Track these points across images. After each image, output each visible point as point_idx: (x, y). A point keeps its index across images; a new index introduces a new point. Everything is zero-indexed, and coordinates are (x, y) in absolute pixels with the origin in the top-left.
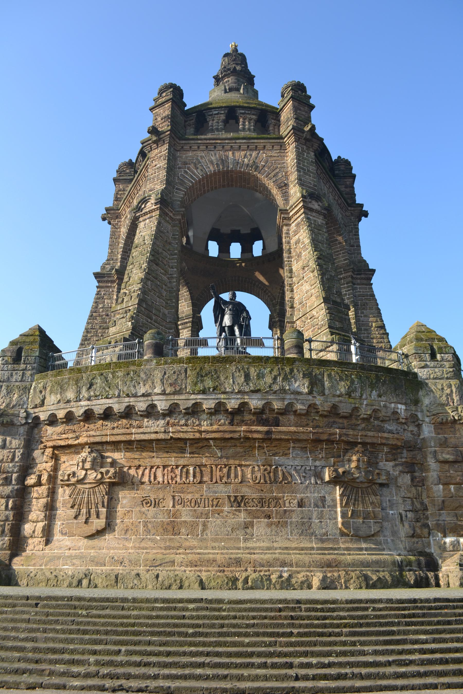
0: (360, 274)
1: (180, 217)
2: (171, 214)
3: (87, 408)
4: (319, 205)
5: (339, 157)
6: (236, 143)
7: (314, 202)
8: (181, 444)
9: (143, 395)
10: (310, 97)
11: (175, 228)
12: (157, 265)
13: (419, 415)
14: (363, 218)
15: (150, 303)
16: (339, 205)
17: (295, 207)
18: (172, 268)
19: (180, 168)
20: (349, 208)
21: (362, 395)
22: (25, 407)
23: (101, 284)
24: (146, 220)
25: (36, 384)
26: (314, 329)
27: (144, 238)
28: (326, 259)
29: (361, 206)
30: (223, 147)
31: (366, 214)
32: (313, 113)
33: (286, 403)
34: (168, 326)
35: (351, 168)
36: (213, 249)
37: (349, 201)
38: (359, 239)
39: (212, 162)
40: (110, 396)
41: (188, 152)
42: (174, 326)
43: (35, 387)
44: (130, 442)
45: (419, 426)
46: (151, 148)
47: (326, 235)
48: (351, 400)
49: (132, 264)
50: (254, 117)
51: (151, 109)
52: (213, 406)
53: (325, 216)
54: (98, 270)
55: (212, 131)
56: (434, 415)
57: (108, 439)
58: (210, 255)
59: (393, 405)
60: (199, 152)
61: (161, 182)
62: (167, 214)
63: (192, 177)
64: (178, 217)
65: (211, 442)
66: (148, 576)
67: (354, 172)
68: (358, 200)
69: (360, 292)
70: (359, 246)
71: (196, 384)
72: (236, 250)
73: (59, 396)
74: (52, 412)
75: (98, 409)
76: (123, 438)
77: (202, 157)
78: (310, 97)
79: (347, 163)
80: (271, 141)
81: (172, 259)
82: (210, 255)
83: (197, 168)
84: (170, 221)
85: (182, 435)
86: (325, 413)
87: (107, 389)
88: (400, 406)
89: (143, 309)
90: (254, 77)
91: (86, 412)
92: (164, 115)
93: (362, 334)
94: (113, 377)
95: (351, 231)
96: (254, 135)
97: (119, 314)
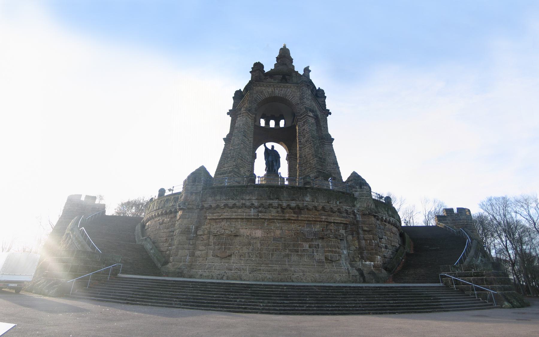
8: (263, 220)
9: (248, 200)
13: (355, 211)
31: (330, 114)
36: (263, 123)
39: (268, 92)
44: (242, 219)
45: (355, 215)
53: (315, 119)
57: (234, 217)
65: (275, 221)
66: (250, 275)
67: (325, 95)
71: (270, 197)
72: (272, 124)
75: (230, 205)
76: (240, 217)
79: (323, 91)
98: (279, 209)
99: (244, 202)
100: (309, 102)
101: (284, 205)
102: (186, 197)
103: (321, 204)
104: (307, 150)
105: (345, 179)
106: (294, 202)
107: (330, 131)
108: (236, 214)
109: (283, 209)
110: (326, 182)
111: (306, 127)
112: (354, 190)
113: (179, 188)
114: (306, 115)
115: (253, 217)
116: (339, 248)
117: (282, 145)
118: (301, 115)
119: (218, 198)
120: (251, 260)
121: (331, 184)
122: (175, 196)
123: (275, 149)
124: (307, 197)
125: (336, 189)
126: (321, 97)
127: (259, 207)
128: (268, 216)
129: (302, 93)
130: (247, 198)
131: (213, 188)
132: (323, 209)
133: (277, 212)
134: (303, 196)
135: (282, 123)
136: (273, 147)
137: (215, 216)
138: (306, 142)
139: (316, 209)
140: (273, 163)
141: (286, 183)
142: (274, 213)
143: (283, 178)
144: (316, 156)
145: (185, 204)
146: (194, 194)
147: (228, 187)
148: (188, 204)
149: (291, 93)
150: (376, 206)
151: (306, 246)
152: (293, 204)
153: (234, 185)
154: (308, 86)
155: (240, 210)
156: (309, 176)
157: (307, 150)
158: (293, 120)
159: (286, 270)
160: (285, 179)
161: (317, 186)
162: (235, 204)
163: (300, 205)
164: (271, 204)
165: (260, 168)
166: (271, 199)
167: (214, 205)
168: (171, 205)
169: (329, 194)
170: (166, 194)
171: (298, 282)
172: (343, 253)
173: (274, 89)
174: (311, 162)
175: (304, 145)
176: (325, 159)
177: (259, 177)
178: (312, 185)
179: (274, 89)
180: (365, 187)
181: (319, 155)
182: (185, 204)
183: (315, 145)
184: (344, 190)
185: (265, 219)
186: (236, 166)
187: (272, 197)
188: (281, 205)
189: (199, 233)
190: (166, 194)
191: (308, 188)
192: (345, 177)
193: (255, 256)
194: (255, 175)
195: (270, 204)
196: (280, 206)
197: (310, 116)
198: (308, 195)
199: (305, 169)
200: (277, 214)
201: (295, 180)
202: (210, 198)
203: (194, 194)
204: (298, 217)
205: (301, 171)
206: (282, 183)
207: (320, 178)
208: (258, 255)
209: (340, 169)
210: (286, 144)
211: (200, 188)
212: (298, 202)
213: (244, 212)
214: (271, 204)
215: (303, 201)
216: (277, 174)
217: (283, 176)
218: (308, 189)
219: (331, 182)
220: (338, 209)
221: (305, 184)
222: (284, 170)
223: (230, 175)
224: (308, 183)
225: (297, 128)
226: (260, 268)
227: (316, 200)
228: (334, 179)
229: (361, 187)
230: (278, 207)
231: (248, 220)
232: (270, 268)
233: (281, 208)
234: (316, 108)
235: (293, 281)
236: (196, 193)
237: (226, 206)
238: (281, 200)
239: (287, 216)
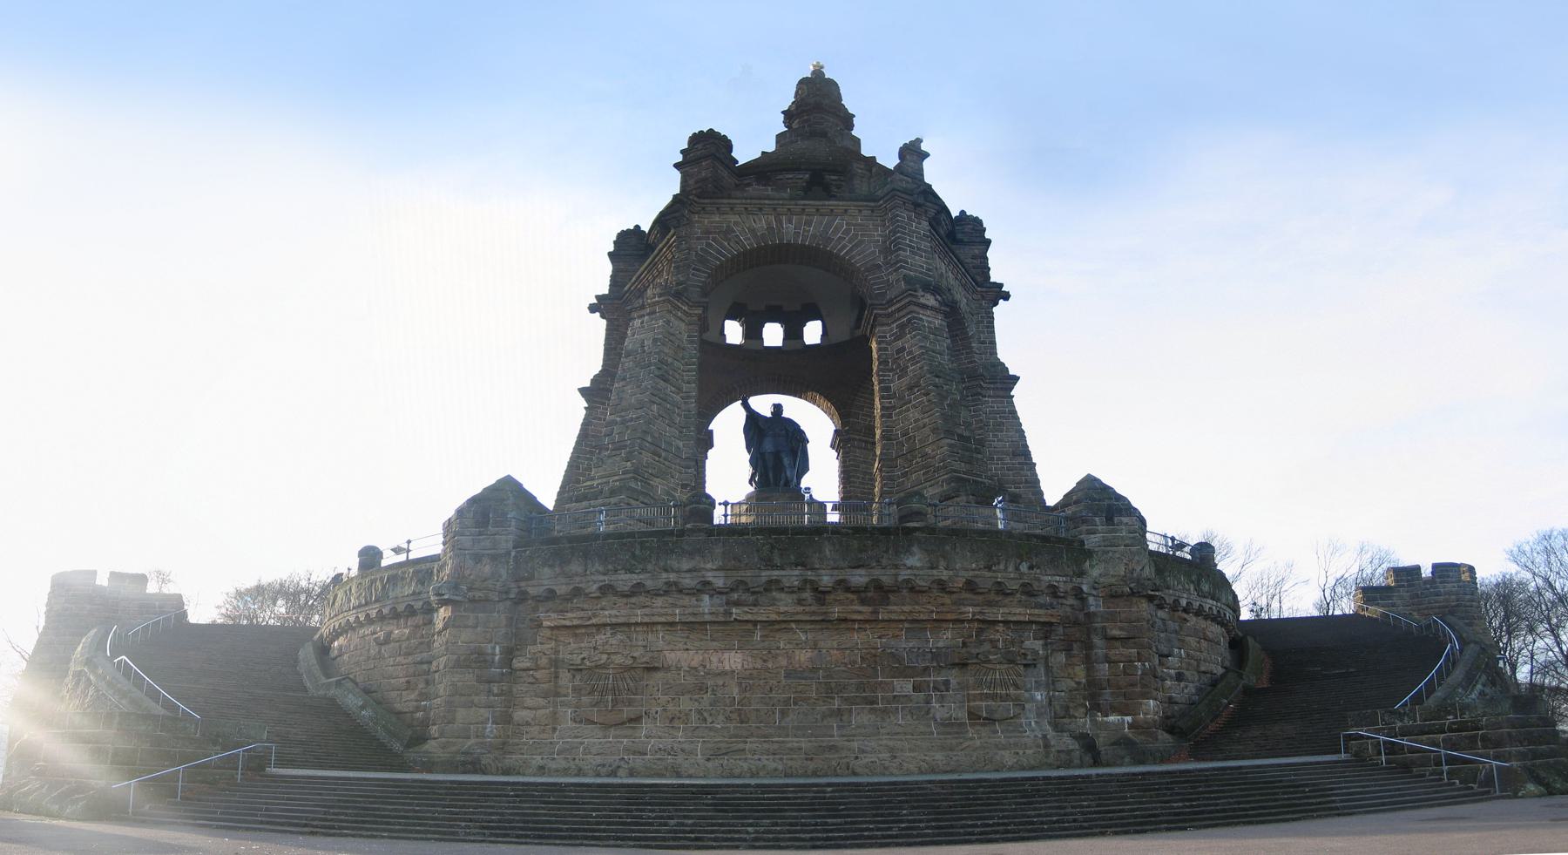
5: (963, 212)
33: (900, 578)
67: (987, 235)
85: (749, 617)
98: (807, 595)
102: (458, 570)
103: (963, 573)
105: (1052, 497)
108: (647, 611)
109: (821, 595)
110: (986, 511)
111: (910, 342)
112: (1084, 528)
115: (708, 618)
116: (1017, 687)
120: (711, 729)
122: (422, 569)
125: (1019, 527)
128: (762, 614)
131: (555, 541)
132: (970, 586)
133: (800, 602)
137: (572, 618)
141: (833, 517)
142: (786, 604)
143: (822, 505)
144: (949, 433)
146: (486, 560)
148: (470, 589)
151: (904, 686)
152: (859, 578)
153: (629, 529)
154: (917, 205)
155: (659, 602)
156: (919, 494)
158: (859, 319)
159: (833, 748)
160: (829, 507)
161: (948, 522)
165: (728, 475)
167: (562, 589)
169: (992, 544)
171: (873, 774)
172: (1032, 699)
176: (981, 442)
177: (726, 504)
178: (931, 519)
180: (1125, 520)
182: (456, 587)
184: (1049, 531)
185: (755, 623)
189: (517, 664)
192: (1054, 487)
193: (721, 717)
194: (709, 497)
200: (800, 609)
201: (867, 509)
202: (546, 570)
203: (486, 560)
204: (876, 612)
205: (888, 479)
206: (817, 518)
207: (962, 499)
208: (735, 716)
209: (1038, 469)
210: (828, 398)
211: (506, 541)
213: (674, 606)
214: (777, 581)
216: (797, 494)
217: (818, 497)
219: (1003, 510)
221: (903, 519)
222: (823, 479)
225: (874, 345)
226: (741, 746)
228: (1014, 499)
229: (1109, 520)
231: (694, 626)
232: (776, 746)
233: (815, 590)
235: (855, 774)
236: (494, 558)
237: (606, 590)
239: (836, 611)
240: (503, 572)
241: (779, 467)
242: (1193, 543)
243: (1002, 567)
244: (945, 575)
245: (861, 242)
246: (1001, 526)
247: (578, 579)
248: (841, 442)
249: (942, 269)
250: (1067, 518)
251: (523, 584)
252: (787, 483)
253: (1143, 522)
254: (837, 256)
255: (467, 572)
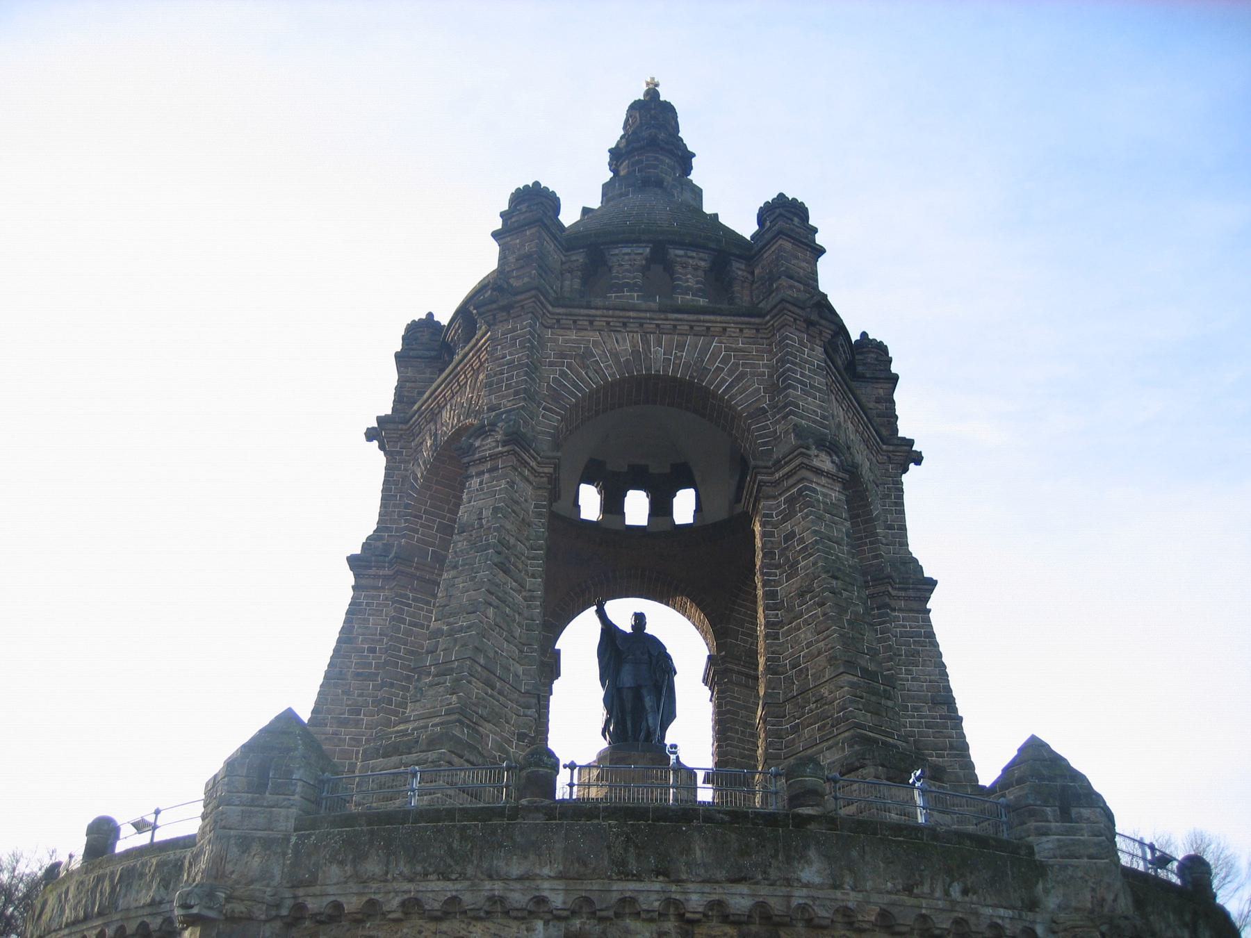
0: (905, 590)
1: (551, 470)
2: (533, 464)
3: (406, 897)
4: (833, 462)
5: (864, 335)
6: (667, 319)
7: (823, 456)
9: (520, 879)
10: (815, 230)
11: (540, 492)
12: (506, 572)
14: (912, 466)
15: (491, 655)
16: (866, 442)
17: (786, 463)
18: (533, 576)
19: (551, 364)
20: (884, 447)
21: (933, 891)
22: (275, 883)
23: (363, 582)
24: (483, 473)
25: (299, 837)
26: (824, 726)
27: (481, 513)
28: (847, 579)
29: (911, 443)
30: (641, 325)
31: (918, 459)
32: (822, 263)
33: (794, 902)
34: (522, 700)
35: (890, 360)
36: (590, 502)
37: (884, 432)
38: (903, 512)
39: (616, 355)
40: (453, 877)
41: (569, 332)
42: (534, 701)
43: (296, 844)
46: (494, 319)
47: (848, 524)
48: (910, 901)
49: (455, 567)
50: (703, 264)
51: (496, 235)
52: (657, 904)
53: (846, 485)
54: (358, 551)
55: (620, 288)
56: (1065, 930)
58: (582, 516)
59: (989, 911)
60: (591, 333)
61: (516, 393)
62: (525, 464)
63: (575, 385)
64: (546, 470)
67: (894, 368)
68: (903, 432)
69: (904, 626)
70: (903, 528)
72: (637, 508)
73: (349, 869)
74: (332, 898)
77: (595, 343)
78: (815, 230)
79: (881, 349)
80: (735, 319)
81: (533, 559)
82: (582, 516)
83: (585, 367)
84: (532, 478)
86: (865, 926)
87: (449, 861)
88: (1002, 912)
89: (479, 669)
90: (694, 155)
91: (403, 904)
92: (522, 252)
93: (909, 717)
94: (462, 837)
95: (889, 496)
96: (702, 302)
97: (429, 674)
99: (498, 887)
100: (816, 403)
101: (696, 900)
102: (218, 861)
103: (875, 898)
104: (806, 635)
105: (987, 772)
106: (743, 888)
107: (919, 546)
110: (899, 793)
111: (800, 524)
112: (1032, 824)
113: (183, 819)
114: (802, 466)
117: (683, 610)
118: (778, 465)
119: (372, 867)
121: (919, 801)
122: (168, 858)
123: (648, 630)
124: (809, 862)
125: (946, 821)
126: (875, 379)
127: (574, 913)
129: (783, 361)
130: (516, 870)
131: (350, 820)
134: (789, 860)
135: (684, 507)
136: (640, 619)
138: (801, 595)
139: (850, 925)
140: (638, 698)
141: (705, 794)
143: (691, 773)
144: (850, 665)
145: (211, 895)
146: (256, 847)
147: (423, 815)
148: (229, 899)
149: (725, 360)
150: (1139, 904)
152: (740, 899)
153: (449, 804)
154: (810, 323)
156: (812, 760)
157: (806, 635)
158: (740, 488)
160: (700, 776)
161: (852, 809)
162: (454, 900)
163: (772, 901)
164: (632, 901)
165: (577, 723)
166: (626, 876)
167: (352, 903)
168: (145, 898)
169: (909, 844)
170: (120, 847)
173: (646, 342)
174: (824, 691)
175: (790, 609)
176: (891, 681)
177: (572, 766)
178: (830, 804)
179: (646, 342)
180: (1086, 812)
181: (864, 661)
182: (211, 895)
183: (842, 610)
184: (985, 829)
186: (462, 711)
187: (633, 866)
188: (677, 903)
190: (120, 847)
191: (811, 818)
192: (989, 761)
194: (551, 754)
195: (623, 901)
196: (674, 907)
197: (819, 472)
198: (812, 853)
199: (795, 729)
201: (747, 782)
202: (335, 869)
203: (256, 847)
205: (775, 736)
206: (684, 795)
207: (870, 770)
209: (967, 727)
210: (701, 606)
211: (286, 819)
212: (764, 890)
214: (632, 901)
215: (788, 882)
216: (659, 754)
217: (687, 761)
218: (812, 826)
219: (923, 792)
220: (957, 922)
221: (795, 800)
222: (692, 735)
223: (432, 755)
224: (813, 794)
225: (757, 528)
227: (848, 880)
228: (936, 775)
229: (1065, 814)
230: (663, 915)
233: (681, 917)
234: (850, 433)
236: (267, 844)
237: (412, 906)
238: (678, 881)
240: (277, 871)
241: (639, 712)
242: (1180, 855)
243: (926, 889)
244: (853, 899)
245: (743, 375)
246: (921, 819)
247: (374, 886)
248: (719, 674)
249: (840, 418)
250: (1007, 806)
251: (301, 892)
252: (649, 735)
253: (1109, 817)
254: (714, 395)
255: (229, 867)
